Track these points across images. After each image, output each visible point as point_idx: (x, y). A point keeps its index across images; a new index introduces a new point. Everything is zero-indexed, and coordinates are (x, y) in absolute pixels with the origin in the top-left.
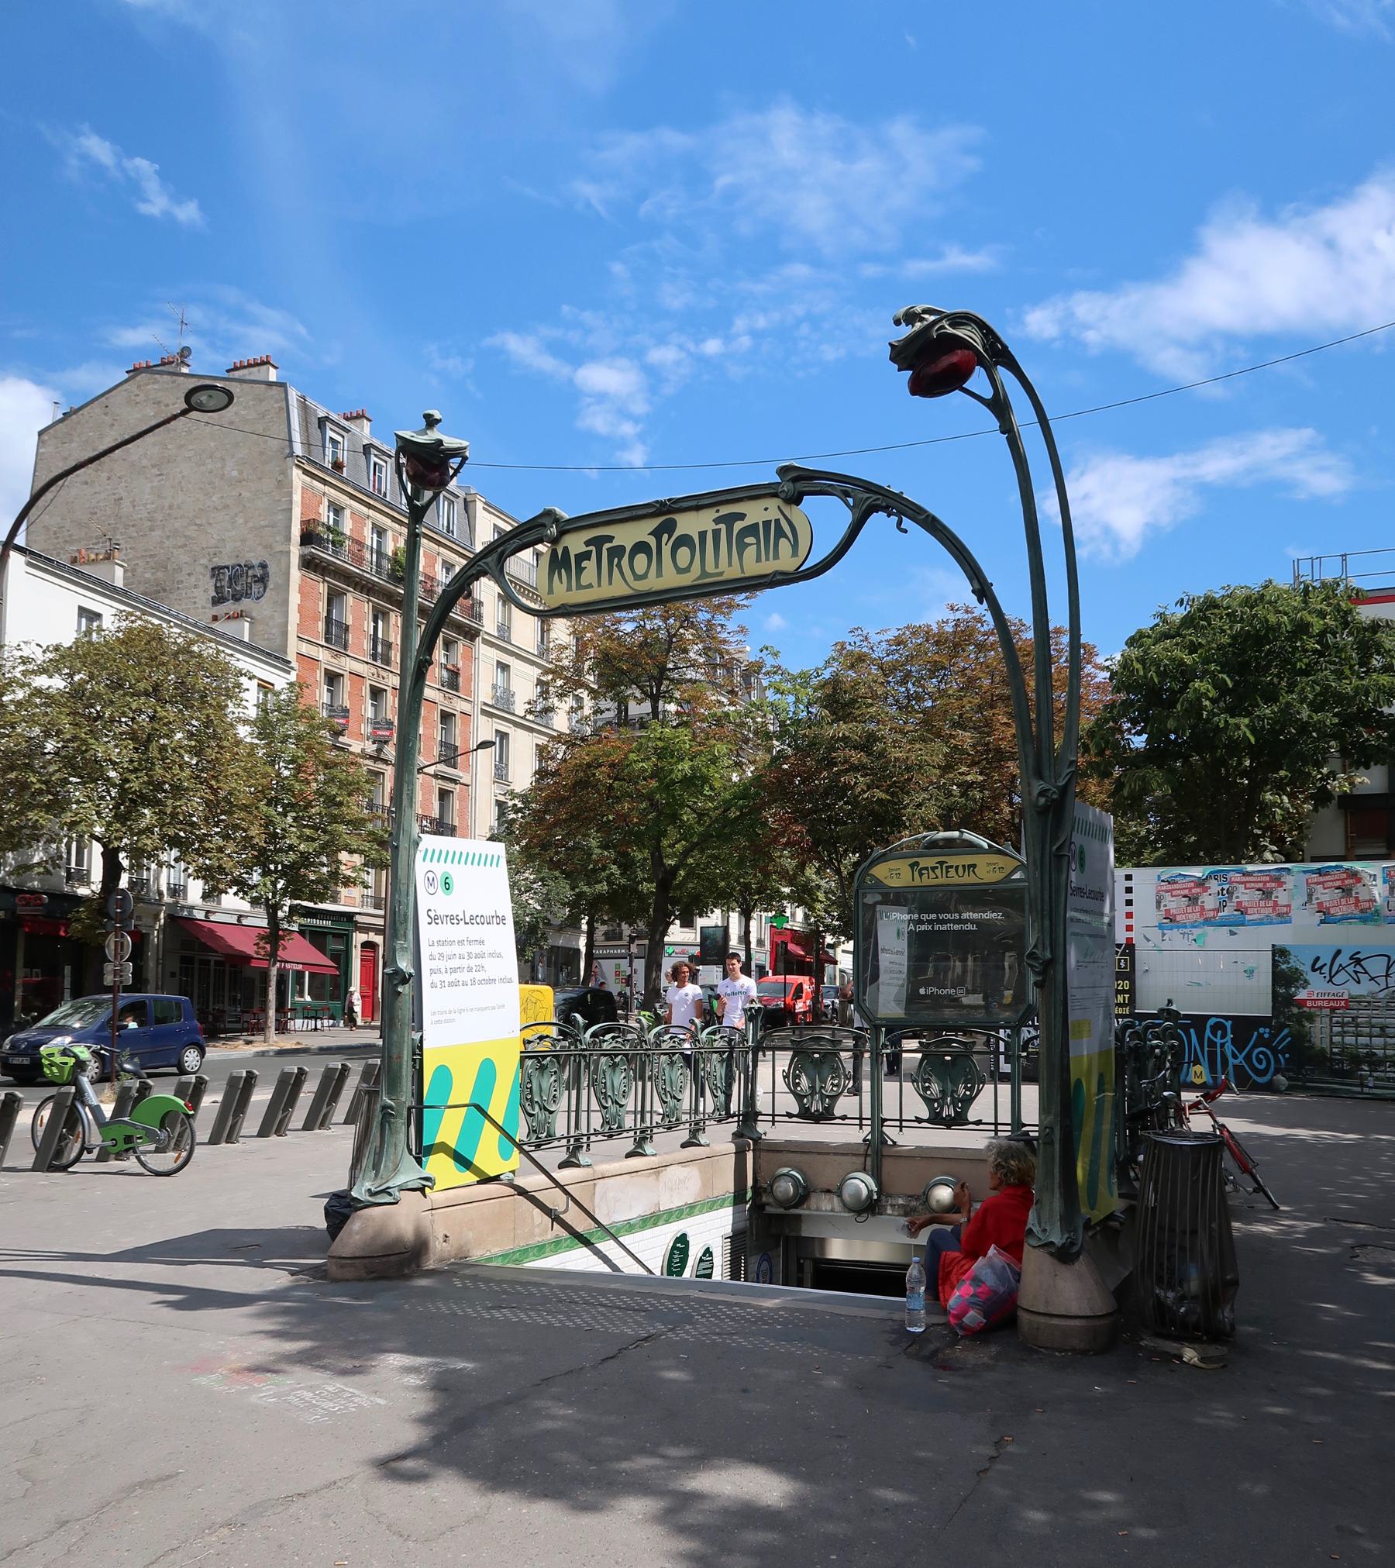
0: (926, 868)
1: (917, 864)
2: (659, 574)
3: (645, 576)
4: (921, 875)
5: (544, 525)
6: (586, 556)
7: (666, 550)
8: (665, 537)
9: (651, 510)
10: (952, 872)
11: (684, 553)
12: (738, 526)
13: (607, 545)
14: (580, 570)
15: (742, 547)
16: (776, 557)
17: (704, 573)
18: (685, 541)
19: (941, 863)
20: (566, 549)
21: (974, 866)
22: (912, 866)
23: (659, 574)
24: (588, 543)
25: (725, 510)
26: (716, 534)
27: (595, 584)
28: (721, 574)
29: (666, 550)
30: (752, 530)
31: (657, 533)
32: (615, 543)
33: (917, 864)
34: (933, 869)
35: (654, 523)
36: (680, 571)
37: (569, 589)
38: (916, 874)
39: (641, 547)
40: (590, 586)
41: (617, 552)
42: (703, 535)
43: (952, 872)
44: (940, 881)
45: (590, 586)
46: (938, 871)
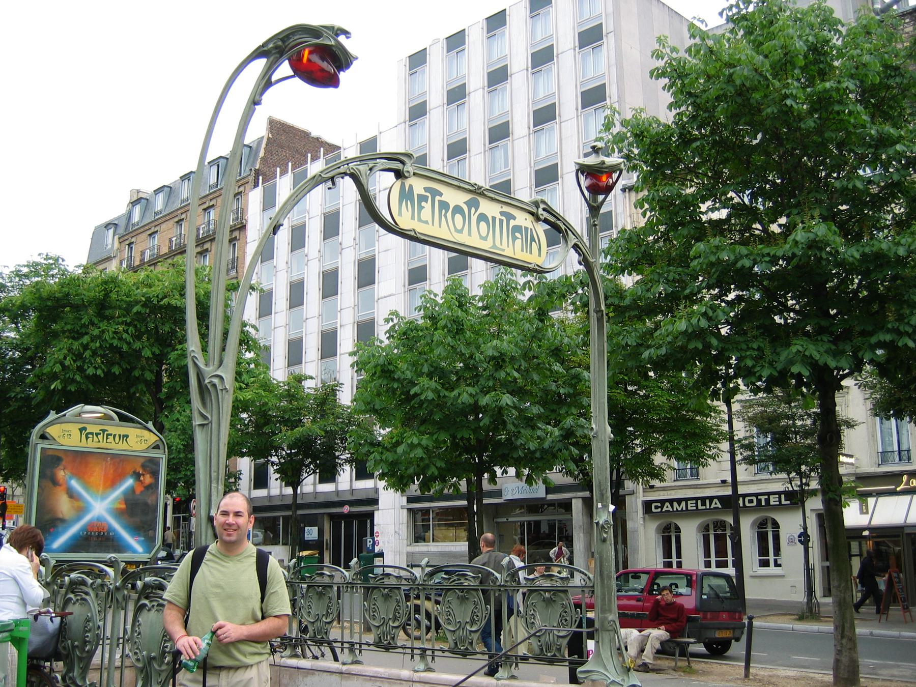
0: (92, 433)
1: (85, 429)
2: (470, 234)
3: (461, 231)
4: (87, 438)
5: (403, 163)
6: (425, 199)
7: (474, 219)
8: (473, 210)
9: (471, 188)
10: (111, 438)
11: (483, 224)
12: (512, 223)
13: (438, 198)
14: (421, 208)
15: (515, 239)
16: (531, 253)
17: (494, 246)
18: (482, 217)
19: (104, 431)
20: (411, 186)
21: (127, 436)
22: (81, 430)
23: (470, 234)
24: (426, 189)
25: (506, 209)
26: (501, 221)
27: (430, 222)
28: (503, 250)
29: (474, 219)
30: (518, 229)
31: (469, 204)
32: (443, 198)
33: (85, 429)
34: (97, 434)
35: (468, 197)
36: (481, 238)
37: (413, 218)
38: (84, 436)
39: (458, 209)
40: (426, 222)
41: (444, 205)
42: (494, 218)
43: (111, 438)
44: (101, 445)
45: (426, 222)
46: (100, 437)
